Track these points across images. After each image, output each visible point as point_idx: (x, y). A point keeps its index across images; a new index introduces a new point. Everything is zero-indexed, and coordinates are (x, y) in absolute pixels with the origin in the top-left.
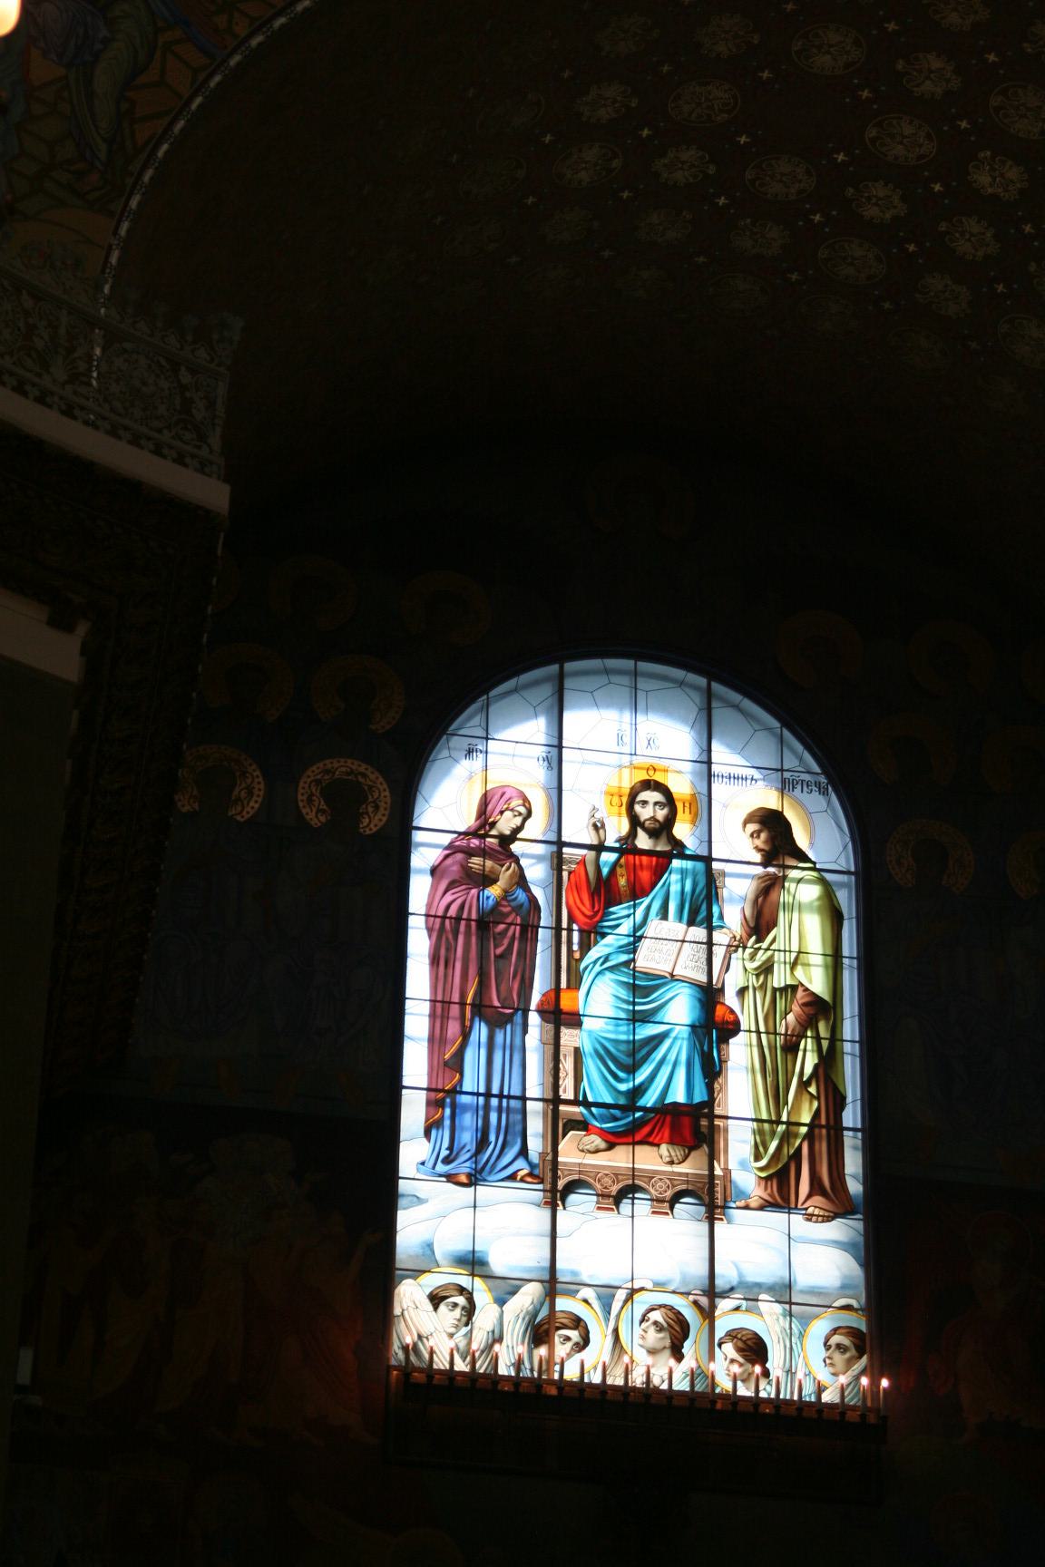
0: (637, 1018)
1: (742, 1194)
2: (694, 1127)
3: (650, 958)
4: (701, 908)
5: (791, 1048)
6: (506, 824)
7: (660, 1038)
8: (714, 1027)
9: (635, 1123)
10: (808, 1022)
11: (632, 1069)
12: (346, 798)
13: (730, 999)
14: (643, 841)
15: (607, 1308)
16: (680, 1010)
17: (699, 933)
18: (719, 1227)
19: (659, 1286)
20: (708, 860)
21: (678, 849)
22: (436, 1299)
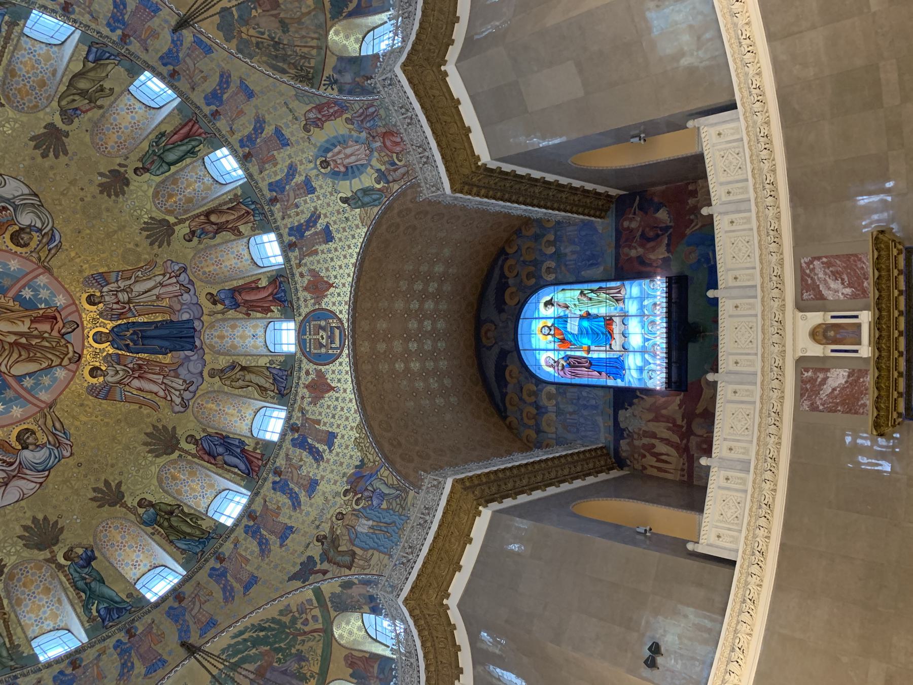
0: (587, 333)
1: (622, 309)
2: (609, 320)
3: (575, 330)
4: (564, 319)
5: (590, 299)
6: (552, 362)
7: (592, 329)
8: (588, 316)
9: (610, 334)
10: (585, 295)
11: (598, 334)
12: (550, 397)
13: (582, 313)
14: (552, 332)
15: (649, 340)
16: (586, 324)
17: (569, 320)
18: (630, 314)
19: (643, 328)
20: (554, 318)
21: (553, 325)
22: (651, 378)
